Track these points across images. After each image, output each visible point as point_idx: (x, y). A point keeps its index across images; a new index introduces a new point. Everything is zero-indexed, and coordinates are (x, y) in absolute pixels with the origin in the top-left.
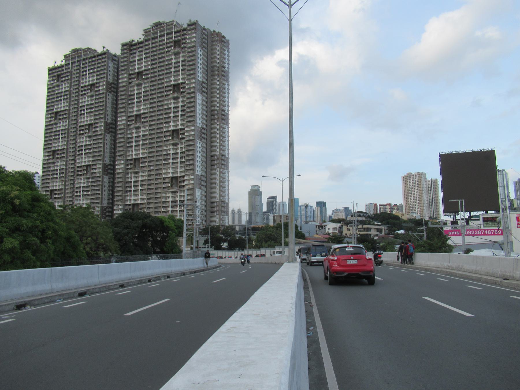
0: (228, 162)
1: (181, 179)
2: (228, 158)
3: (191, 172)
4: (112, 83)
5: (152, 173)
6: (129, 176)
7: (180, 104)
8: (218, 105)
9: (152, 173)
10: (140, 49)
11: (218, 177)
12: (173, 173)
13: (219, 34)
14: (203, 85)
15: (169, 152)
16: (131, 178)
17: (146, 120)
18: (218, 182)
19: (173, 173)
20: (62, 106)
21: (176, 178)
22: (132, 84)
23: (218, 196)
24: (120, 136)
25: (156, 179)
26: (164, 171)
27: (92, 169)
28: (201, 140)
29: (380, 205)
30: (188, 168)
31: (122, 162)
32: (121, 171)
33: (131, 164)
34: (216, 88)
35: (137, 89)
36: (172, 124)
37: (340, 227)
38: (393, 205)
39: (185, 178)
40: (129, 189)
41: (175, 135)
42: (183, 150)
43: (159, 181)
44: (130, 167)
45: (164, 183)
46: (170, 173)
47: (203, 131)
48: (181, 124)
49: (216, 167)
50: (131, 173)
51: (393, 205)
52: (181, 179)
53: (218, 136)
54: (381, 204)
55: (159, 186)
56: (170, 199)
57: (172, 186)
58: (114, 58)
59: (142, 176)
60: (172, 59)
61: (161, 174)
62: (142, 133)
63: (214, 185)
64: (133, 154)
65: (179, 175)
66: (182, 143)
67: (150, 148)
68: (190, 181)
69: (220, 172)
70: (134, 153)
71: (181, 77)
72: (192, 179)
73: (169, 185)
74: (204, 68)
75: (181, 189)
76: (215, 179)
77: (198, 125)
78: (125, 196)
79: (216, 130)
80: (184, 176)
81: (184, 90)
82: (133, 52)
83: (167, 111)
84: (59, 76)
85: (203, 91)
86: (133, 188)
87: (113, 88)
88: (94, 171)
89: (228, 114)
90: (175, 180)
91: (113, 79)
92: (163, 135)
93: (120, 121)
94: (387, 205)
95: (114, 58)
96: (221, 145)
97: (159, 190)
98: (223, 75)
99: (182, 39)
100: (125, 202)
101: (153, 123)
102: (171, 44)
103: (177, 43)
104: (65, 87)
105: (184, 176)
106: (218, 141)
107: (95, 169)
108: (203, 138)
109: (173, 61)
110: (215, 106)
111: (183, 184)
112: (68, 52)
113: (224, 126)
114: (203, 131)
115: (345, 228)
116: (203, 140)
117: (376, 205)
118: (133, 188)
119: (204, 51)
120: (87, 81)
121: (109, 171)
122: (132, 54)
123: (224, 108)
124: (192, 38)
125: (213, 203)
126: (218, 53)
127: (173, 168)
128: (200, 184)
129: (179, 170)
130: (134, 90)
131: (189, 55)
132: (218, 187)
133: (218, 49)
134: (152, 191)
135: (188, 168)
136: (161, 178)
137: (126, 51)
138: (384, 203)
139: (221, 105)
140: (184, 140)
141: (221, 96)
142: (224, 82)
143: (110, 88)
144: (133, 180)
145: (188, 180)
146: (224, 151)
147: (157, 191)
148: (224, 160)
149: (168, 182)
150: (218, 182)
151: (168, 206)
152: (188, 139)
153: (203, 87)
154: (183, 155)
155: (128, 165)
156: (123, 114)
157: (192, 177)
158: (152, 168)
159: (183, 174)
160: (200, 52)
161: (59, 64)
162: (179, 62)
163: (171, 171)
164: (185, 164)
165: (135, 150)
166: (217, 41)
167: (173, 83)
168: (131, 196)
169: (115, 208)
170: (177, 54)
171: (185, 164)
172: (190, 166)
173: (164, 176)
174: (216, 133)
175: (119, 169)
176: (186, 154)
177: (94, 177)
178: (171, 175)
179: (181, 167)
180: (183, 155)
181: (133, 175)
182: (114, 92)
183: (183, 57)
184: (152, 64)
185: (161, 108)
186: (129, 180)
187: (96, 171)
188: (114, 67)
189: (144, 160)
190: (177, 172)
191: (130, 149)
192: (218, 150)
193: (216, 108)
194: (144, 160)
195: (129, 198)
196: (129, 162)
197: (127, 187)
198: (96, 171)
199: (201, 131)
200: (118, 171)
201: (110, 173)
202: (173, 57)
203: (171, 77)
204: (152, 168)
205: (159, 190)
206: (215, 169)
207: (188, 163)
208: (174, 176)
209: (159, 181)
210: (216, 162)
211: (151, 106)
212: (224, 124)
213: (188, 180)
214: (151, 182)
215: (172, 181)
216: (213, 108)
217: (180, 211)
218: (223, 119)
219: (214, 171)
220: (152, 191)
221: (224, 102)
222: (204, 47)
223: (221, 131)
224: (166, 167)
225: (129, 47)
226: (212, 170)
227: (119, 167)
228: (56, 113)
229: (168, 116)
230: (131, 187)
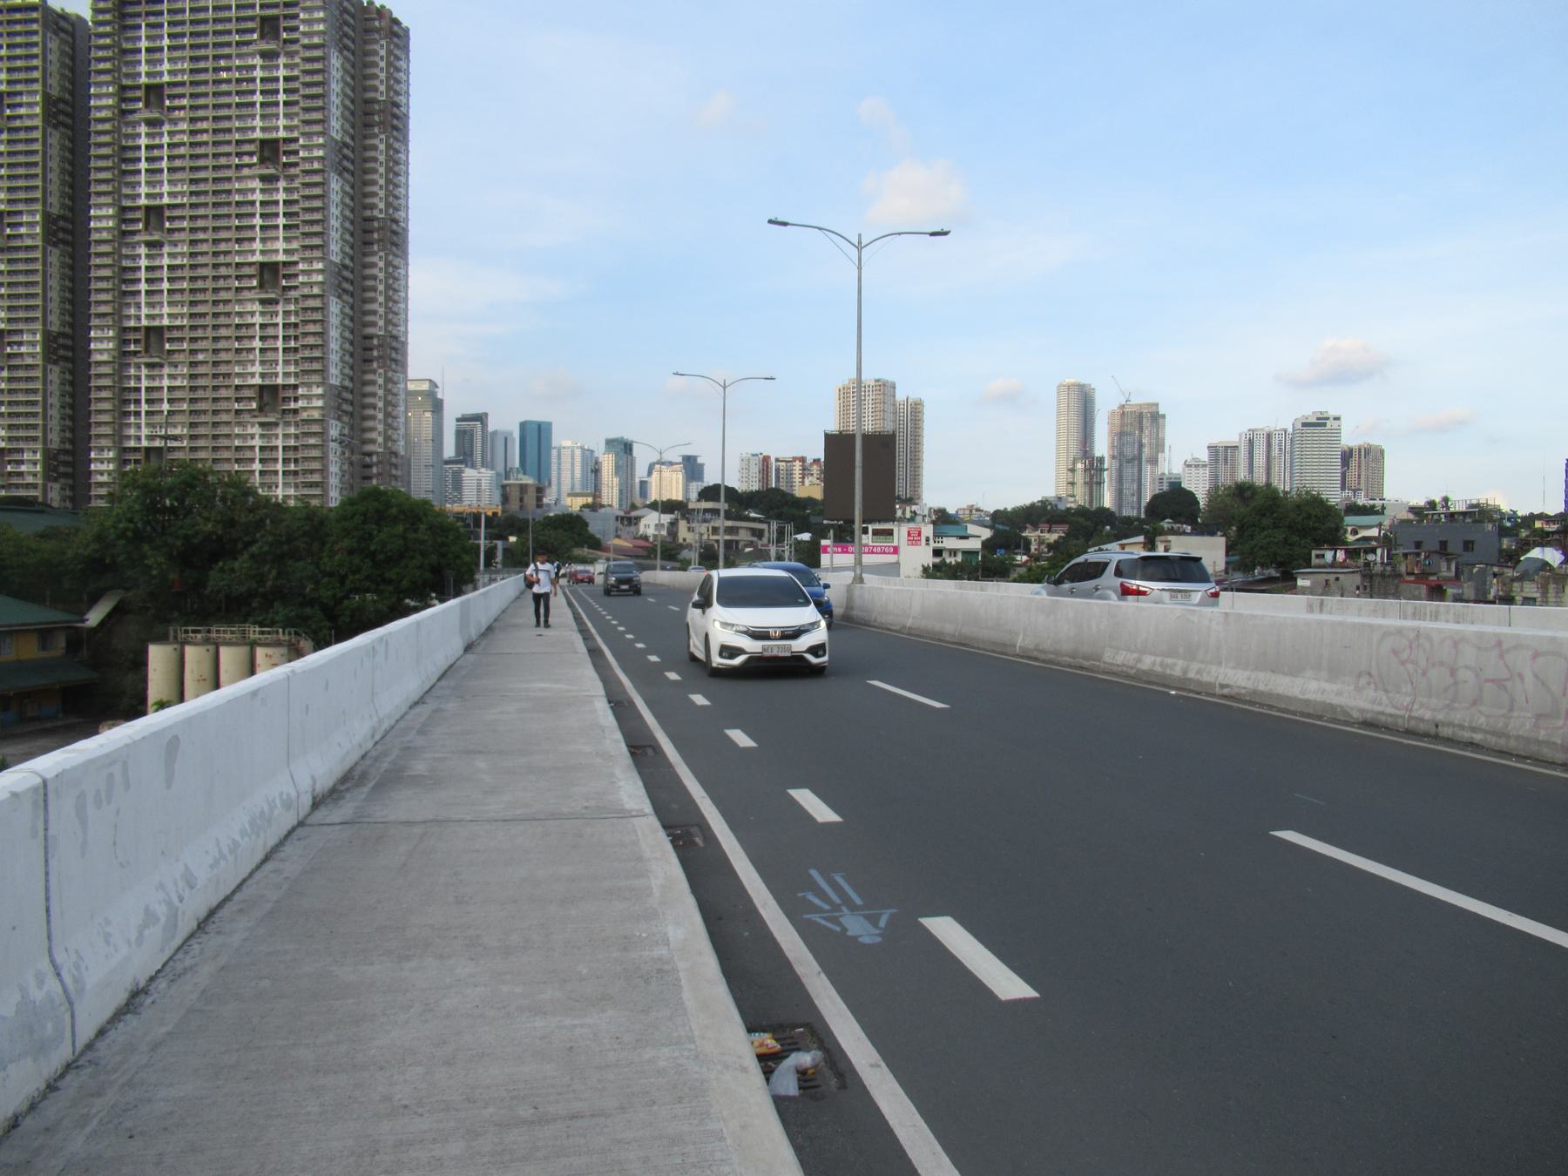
0: (405, 354)
1: (289, 394)
2: (405, 344)
3: (316, 378)
4: (61, 100)
5: (201, 370)
6: (132, 371)
7: (281, 196)
8: (382, 206)
9: (201, 370)
10: (152, 19)
11: (381, 392)
12: (263, 375)
13: (382, 12)
14: (346, 151)
15: (250, 321)
16: (138, 378)
17: (177, 225)
18: (381, 404)
19: (263, 375)
21: (274, 389)
22: (131, 118)
23: (380, 440)
24: (98, 261)
25: (215, 388)
26: (237, 369)
27: (10, 344)
28: (339, 297)
29: (777, 460)
30: (306, 366)
31: (111, 333)
32: (105, 357)
33: (137, 341)
34: (375, 160)
35: (147, 135)
36: (257, 245)
37: (674, 524)
38: (809, 461)
39: (300, 391)
40: (132, 408)
41: (266, 276)
42: (293, 319)
43: (223, 393)
44: (132, 348)
45: (238, 400)
46: (255, 374)
47: (346, 273)
48: (286, 252)
49: (375, 365)
50: (138, 367)
51: (809, 461)
52: (289, 394)
53: (381, 288)
54: (781, 456)
55: (223, 405)
56: (257, 442)
57: (261, 409)
58: (63, 24)
59: (171, 376)
60: (253, 67)
61: (229, 375)
62: (166, 261)
63: (370, 412)
64: (141, 314)
65: (280, 381)
66: (288, 301)
67: (193, 303)
68: (312, 400)
69: (388, 380)
70: (144, 311)
71: (282, 122)
72: (319, 396)
73: (254, 405)
74: (345, 107)
75: (290, 418)
76: (374, 395)
77: (333, 258)
78: (123, 426)
79: (375, 271)
80: (295, 387)
81: (293, 159)
82: (130, 22)
83: (244, 210)
85: (345, 169)
86: (144, 407)
87: (67, 112)
88: (15, 349)
89: (406, 230)
90: (269, 396)
91: (63, 88)
92: (232, 272)
93: (99, 218)
94: (795, 459)
95: (61, 24)
96: (389, 310)
97: (224, 417)
98: (395, 128)
99: (286, 17)
100: (121, 442)
101: (201, 236)
102: (250, 25)
105: (295, 387)
106: (381, 299)
107: (20, 344)
108: (345, 291)
109: (258, 74)
110: (373, 207)
111: (292, 405)
113: (396, 262)
114: (346, 273)
115: (683, 525)
116: (345, 297)
117: (766, 459)
118: (144, 407)
119: (346, 58)
121: (61, 352)
122: (125, 28)
123: (396, 216)
125: (370, 454)
126: (383, 64)
127: (263, 363)
128: (339, 408)
129: (280, 369)
130: (139, 135)
131: (308, 67)
132: (380, 416)
133: (383, 53)
134: (203, 419)
135: (306, 366)
136: (227, 387)
137: (108, 17)
138: (789, 455)
139: (388, 205)
140: (293, 294)
141: (388, 181)
142: (397, 145)
143: (55, 115)
144: (144, 383)
145: (309, 397)
146: (396, 325)
147: (217, 419)
148: (395, 349)
149: (250, 399)
150: (381, 404)
151: (252, 460)
152: (306, 291)
153: (345, 157)
154: (291, 332)
155: (126, 342)
156: (108, 200)
157: (320, 391)
158: (201, 357)
159: (292, 381)
160: (336, 61)
162: (276, 79)
163: (257, 368)
164: (299, 356)
165: (149, 305)
166: (378, 31)
167: (258, 135)
168: (139, 426)
169: (93, 455)
170: (267, 55)
171: (299, 356)
172: (314, 365)
173: (237, 382)
174: (375, 278)
175: (101, 351)
176: (301, 330)
177: (17, 367)
178: (257, 381)
179: (286, 362)
180: (291, 332)
181: (144, 371)
182: (66, 126)
183: (286, 66)
184: (192, 71)
185: (223, 198)
186: (133, 384)
187: (23, 349)
188: (62, 52)
189: (176, 334)
190: (276, 375)
191: (129, 300)
192: (381, 323)
193: (376, 213)
194: (176, 334)
195: (132, 432)
196: (132, 336)
197: (127, 402)
198: (23, 349)
199: (339, 274)
200: (99, 358)
201: (66, 359)
202: (258, 61)
203: (253, 117)
204: (201, 357)
205: (224, 417)
206: (374, 372)
207: (307, 354)
208: (267, 382)
209: (223, 393)
210: (375, 353)
211: (193, 188)
212: (396, 256)
213: (309, 397)
214: (200, 394)
215: (261, 397)
216: (368, 213)
217: (284, 473)
218: (396, 245)
219: (369, 377)
220: (203, 419)
221: (397, 198)
222: (346, 47)
223: (389, 275)
224: (244, 355)
226: (364, 372)
227: (100, 346)
229: (245, 222)
230: (138, 402)
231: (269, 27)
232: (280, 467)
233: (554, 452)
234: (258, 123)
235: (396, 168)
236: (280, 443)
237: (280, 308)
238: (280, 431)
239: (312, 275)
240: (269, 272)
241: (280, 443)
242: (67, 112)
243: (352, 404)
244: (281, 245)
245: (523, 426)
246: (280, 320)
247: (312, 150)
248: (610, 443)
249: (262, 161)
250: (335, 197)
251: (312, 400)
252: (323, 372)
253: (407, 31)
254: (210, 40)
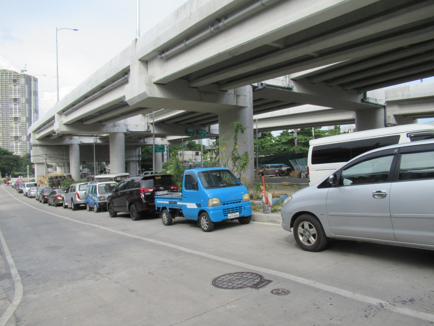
7: (18, 107)
21: (17, 137)
36: (14, 114)
57: (15, 140)
90: (16, 138)
103: (15, 81)
163: (14, 134)
178: (14, 135)
231: (15, 81)
232: (19, 149)
234: (13, 95)
235: (36, 101)
236: (19, 145)
237: (18, 124)
238: (19, 143)
240: (16, 119)
241: (19, 145)
244: (18, 114)
246: (18, 126)
249: (14, 102)
250: (27, 107)
253: (37, 79)
254: (4, 82)
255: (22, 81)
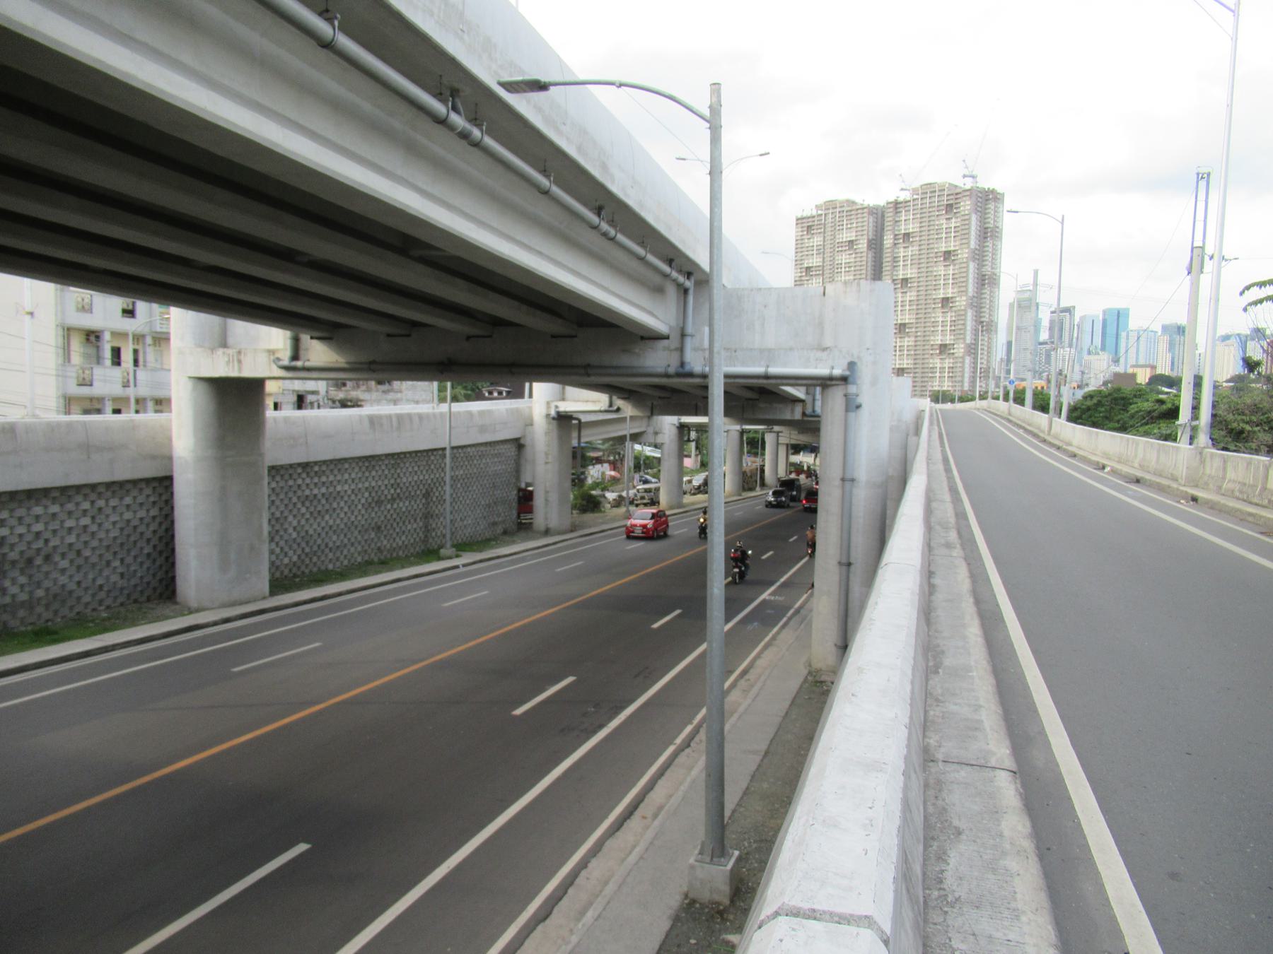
13: (993, 191)
20: (815, 261)
21: (945, 345)
46: (938, 340)
68: (959, 349)
84: (809, 227)
90: (944, 348)
103: (949, 207)
104: (817, 240)
112: (821, 201)
120: (846, 236)
124: (966, 205)
161: (807, 213)
225: (896, 205)
228: (808, 268)
233: (1123, 334)
239: (961, 302)
240: (946, 301)
242: (876, 244)
243: (972, 350)
244: (950, 290)
245: (1104, 312)
247: (964, 254)
248: (1165, 328)
251: (959, 349)
252: (964, 339)
255: (966, 205)
